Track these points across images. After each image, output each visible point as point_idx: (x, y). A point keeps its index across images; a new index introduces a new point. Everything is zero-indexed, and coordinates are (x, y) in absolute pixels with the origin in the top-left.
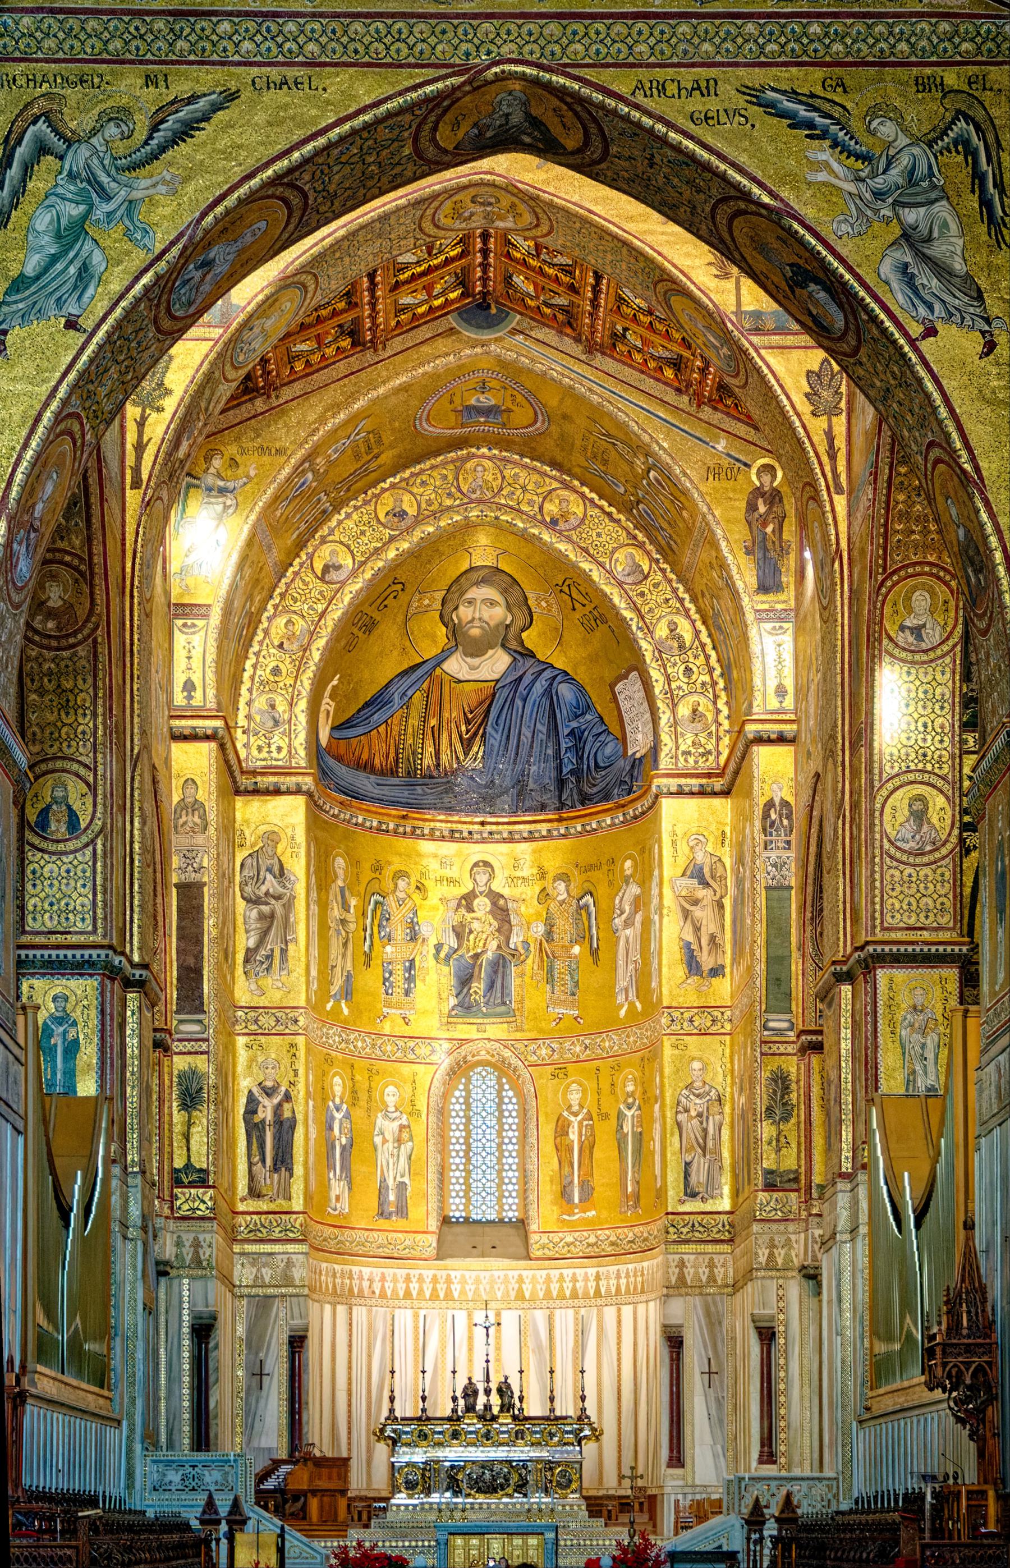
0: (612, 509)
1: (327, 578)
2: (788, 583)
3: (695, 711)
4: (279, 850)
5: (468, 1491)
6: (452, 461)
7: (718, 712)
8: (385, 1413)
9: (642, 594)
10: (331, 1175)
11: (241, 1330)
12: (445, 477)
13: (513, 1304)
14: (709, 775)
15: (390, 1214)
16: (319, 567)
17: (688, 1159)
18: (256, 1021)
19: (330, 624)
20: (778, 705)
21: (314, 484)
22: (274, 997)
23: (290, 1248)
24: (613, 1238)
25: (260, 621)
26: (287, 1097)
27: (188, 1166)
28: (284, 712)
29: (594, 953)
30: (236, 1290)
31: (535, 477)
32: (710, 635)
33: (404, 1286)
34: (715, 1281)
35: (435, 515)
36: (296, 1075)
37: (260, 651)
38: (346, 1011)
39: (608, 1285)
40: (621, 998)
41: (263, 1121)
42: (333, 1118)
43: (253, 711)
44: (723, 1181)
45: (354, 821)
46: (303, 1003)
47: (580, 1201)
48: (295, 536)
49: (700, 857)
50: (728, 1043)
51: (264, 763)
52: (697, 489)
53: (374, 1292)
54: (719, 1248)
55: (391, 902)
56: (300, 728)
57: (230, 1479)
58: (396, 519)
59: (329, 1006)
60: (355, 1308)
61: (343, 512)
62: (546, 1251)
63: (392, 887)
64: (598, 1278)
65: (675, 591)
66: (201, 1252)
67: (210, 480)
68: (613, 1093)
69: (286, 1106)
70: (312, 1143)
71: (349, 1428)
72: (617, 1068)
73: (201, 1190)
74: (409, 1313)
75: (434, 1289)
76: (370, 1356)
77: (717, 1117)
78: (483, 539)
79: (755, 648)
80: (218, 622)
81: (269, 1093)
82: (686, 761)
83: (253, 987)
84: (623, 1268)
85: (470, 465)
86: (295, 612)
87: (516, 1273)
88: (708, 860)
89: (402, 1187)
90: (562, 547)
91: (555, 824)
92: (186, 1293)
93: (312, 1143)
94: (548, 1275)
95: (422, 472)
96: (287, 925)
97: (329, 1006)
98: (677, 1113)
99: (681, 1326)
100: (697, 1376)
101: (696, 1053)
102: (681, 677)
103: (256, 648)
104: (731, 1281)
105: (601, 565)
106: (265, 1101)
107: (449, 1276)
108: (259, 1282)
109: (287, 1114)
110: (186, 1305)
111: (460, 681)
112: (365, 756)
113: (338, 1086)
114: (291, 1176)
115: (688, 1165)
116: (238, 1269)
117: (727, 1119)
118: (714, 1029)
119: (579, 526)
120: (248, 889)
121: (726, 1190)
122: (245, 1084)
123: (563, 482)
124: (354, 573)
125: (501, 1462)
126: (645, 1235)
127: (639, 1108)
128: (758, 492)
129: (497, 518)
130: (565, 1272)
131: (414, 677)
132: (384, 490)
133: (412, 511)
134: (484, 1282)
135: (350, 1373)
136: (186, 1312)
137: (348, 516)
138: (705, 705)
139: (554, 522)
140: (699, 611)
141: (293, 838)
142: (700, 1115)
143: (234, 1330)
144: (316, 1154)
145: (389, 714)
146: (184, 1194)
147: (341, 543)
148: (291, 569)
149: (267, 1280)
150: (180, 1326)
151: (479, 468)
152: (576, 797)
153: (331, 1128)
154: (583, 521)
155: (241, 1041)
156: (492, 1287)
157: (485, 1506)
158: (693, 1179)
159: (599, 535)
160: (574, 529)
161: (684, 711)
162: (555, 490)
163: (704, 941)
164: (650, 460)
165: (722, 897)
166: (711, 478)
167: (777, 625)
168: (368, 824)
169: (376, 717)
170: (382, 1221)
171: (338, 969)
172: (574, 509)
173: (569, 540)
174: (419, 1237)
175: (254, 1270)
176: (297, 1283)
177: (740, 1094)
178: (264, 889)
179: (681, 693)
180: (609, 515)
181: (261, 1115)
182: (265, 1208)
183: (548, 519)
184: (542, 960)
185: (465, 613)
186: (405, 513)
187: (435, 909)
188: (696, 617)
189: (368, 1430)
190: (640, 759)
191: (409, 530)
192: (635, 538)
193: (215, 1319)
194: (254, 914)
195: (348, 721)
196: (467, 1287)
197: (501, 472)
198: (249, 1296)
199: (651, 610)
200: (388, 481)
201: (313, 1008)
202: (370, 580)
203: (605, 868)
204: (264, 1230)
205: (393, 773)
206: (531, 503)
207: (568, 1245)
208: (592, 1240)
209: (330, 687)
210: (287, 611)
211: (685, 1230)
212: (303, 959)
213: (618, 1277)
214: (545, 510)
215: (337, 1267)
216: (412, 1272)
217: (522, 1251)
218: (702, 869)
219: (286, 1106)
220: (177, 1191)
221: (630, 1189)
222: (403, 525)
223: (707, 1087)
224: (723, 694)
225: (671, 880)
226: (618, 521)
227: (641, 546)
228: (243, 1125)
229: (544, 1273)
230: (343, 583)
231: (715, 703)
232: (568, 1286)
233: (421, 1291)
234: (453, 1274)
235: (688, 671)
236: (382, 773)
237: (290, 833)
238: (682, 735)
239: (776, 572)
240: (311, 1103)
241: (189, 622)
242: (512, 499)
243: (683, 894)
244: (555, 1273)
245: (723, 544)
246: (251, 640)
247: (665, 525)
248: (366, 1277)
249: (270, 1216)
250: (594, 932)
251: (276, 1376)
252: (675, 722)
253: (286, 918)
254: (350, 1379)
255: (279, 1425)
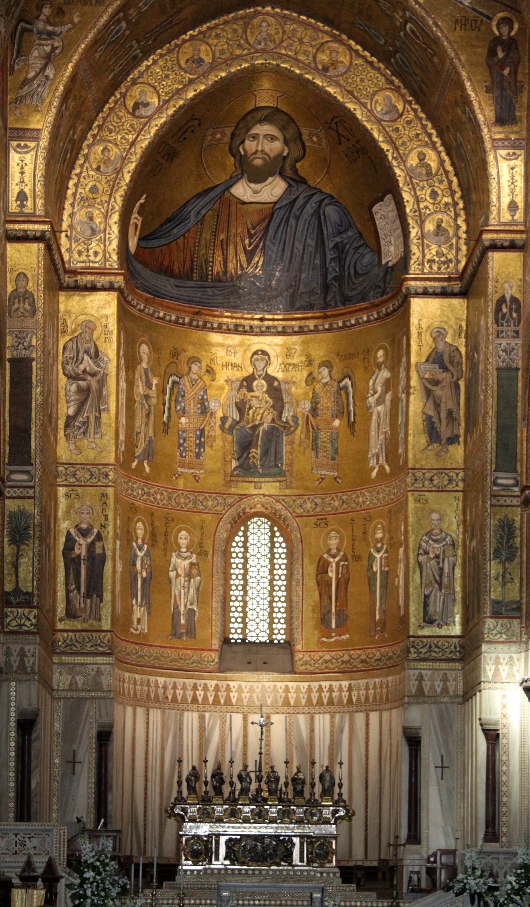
0: (374, 59)
1: (137, 113)
2: (521, 117)
3: (439, 226)
4: (95, 336)
5: (244, 859)
6: (242, 18)
7: (458, 227)
8: (175, 795)
9: (397, 130)
10: (134, 602)
11: (58, 726)
12: (235, 31)
13: (280, 710)
14: (449, 279)
15: (182, 634)
16: (130, 104)
17: (427, 592)
18: (74, 475)
19: (139, 151)
20: (510, 218)
21: (128, 32)
22: (90, 455)
23: (100, 659)
24: (363, 657)
25: (81, 148)
26: (99, 537)
27: (17, 590)
28: (100, 223)
29: (352, 426)
30: (54, 693)
31: (310, 32)
32: (453, 164)
33: (192, 693)
34: (448, 692)
35: (228, 63)
36: (106, 519)
37: (81, 173)
38: (147, 469)
39: (359, 695)
40: (373, 462)
41: (79, 556)
42: (136, 556)
43: (75, 222)
44: (456, 610)
45: (156, 315)
46: (112, 460)
47: (337, 626)
48: (111, 77)
49: (441, 347)
50: (461, 498)
51: (83, 265)
52: (447, 38)
53: (167, 698)
54: (451, 665)
55: (186, 381)
56: (113, 236)
57: (47, 846)
58: (194, 66)
59: (134, 465)
60: (151, 711)
61: (151, 59)
62: (308, 667)
63: (186, 369)
64: (350, 689)
65: (424, 127)
66: (26, 660)
67: (40, 25)
68: (366, 539)
69: (98, 544)
70: (118, 575)
71: (145, 807)
72: (369, 519)
73: (27, 610)
74: (195, 715)
75: (216, 697)
76: (163, 749)
77: (452, 559)
78: (266, 84)
79: (493, 171)
80: (46, 144)
81: (84, 533)
82: (431, 267)
83: (72, 447)
84: (371, 681)
85: (255, 21)
86: (110, 141)
87: (283, 684)
88: (448, 349)
89: (190, 613)
90: (331, 90)
91: (321, 321)
92: (13, 694)
93: (118, 575)
94: (309, 686)
95: (216, 26)
96: (100, 397)
97: (134, 465)
98: (418, 555)
99: (419, 728)
100: (432, 769)
101: (436, 507)
102: (428, 198)
103: (77, 171)
104: (460, 692)
105: (364, 105)
106: (81, 540)
107: (228, 685)
108: (74, 688)
109: (98, 551)
110: (13, 704)
111: (244, 203)
112: (166, 264)
113: (140, 529)
114: (101, 601)
115: (427, 597)
116: (56, 676)
117: (460, 561)
118: (450, 487)
119: (345, 73)
120: (69, 367)
121: (458, 618)
122: (64, 526)
123: (333, 36)
124: (159, 110)
125: (270, 836)
126: (390, 654)
127: (387, 551)
128: (497, 41)
129: (278, 65)
130: (323, 684)
131: (207, 199)
132: (185, 41)
133: (208, 59)
134: (257, 691)
135: (146, 763)
136: (13, 709)
137: (155, 62)
138: (446, 219)
139: (326, 69)
140: (443, 144)
141: (106, 326)
142: (437, 557)
143: (52, 725)
144: (122, 585)
145: (186, 229)
146: (12, 613)
147: (149, 84)
148: (107, 106)
149: (80, 685)
150: (8, 721)
151: (264, 24)
152: (338, 298)
153: (134, 564)
154: (348, 69)
155: (62, 491)
156: (263, 696)
157: (257, 872)
158: (431, 609)
159: (362, 80)
160: (342, 75)
161: (430, 227)
162: (327, 42)
163: (443, 415)
164: (408, 14)
165: (458, 379)
166: (458, 28)
167: (511, 151)
168: (168, 318)
169: (175, 230)
170: (175, 640)
171: (142, 435)
172: (342, 59)
173: (338, 84)
174: (205, 653)
175: (70, 677)
176: (105, 688)
177: (471, 540)
178: (82, 367)
179: (428, 212)
180: (371, 63)
181: (77, 551)
182: (79, 627)
183: (320, 67)
184: (308, 430)
185: (250, 146)
186: (202, 60)
187: (222, 388)
188: (441, 149)
189: (161, 810)
190: (392, 267)
191: (205, 75)
192: (392, 82)
193: (37, 715)
194: (74, 388)
195: (152, 234)
196: (243, 695)
197: (283, 27)
198: (65, 698)
199: (404, 143)
200: (188, 33)
201: (122, 466)
202: (173, 116)
203: (361, 356)
204: (78, 645)
205: (189, 278)
206: (305, 53)
207: (326, 662)
208: (346, 658)
209: (138, 204)
210: (103, 140)
211: (424, 650)
212: (113, 425)
213: (367, 688)
214: (318, 59)
215: (138, 677)
216: (198, 682)
217: (288, 667)
218: (442, 356)
219: (98, 544)
220: (7, 610)
221: (378, 617)
222: (200, 70)
223: (444, 534)
224: (462, 213)
225: (416, 365)
226: (378, 69)
227: (397, 89)
228: (62, 559)
229: (306, 684)
230: (150, 118)
231: (455, 220)
232: (325, 695)
233: (205, 698)
234: (231, 684)
235: (434, 194)
236: (179, 277)
237: (103, 321)
238: (428, 246)
239: (511, 108)
240: (118, 543)
241: (22, 143)
242: (291, 50)
243: (427, 376)
244: (315, 685)
245: (468, 84)
246: (74, 163)
247: (418, 71)
248: (161, 686)
249: (83, 634)
250: (352, 408)
251: (86, 764)
252: (423, 237)
253: (100, 392)
254: (146, 767)
255: (88, 803)
